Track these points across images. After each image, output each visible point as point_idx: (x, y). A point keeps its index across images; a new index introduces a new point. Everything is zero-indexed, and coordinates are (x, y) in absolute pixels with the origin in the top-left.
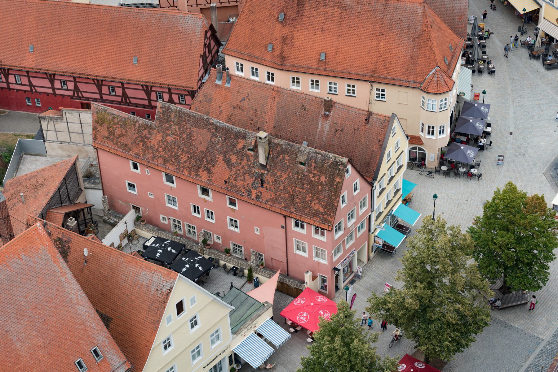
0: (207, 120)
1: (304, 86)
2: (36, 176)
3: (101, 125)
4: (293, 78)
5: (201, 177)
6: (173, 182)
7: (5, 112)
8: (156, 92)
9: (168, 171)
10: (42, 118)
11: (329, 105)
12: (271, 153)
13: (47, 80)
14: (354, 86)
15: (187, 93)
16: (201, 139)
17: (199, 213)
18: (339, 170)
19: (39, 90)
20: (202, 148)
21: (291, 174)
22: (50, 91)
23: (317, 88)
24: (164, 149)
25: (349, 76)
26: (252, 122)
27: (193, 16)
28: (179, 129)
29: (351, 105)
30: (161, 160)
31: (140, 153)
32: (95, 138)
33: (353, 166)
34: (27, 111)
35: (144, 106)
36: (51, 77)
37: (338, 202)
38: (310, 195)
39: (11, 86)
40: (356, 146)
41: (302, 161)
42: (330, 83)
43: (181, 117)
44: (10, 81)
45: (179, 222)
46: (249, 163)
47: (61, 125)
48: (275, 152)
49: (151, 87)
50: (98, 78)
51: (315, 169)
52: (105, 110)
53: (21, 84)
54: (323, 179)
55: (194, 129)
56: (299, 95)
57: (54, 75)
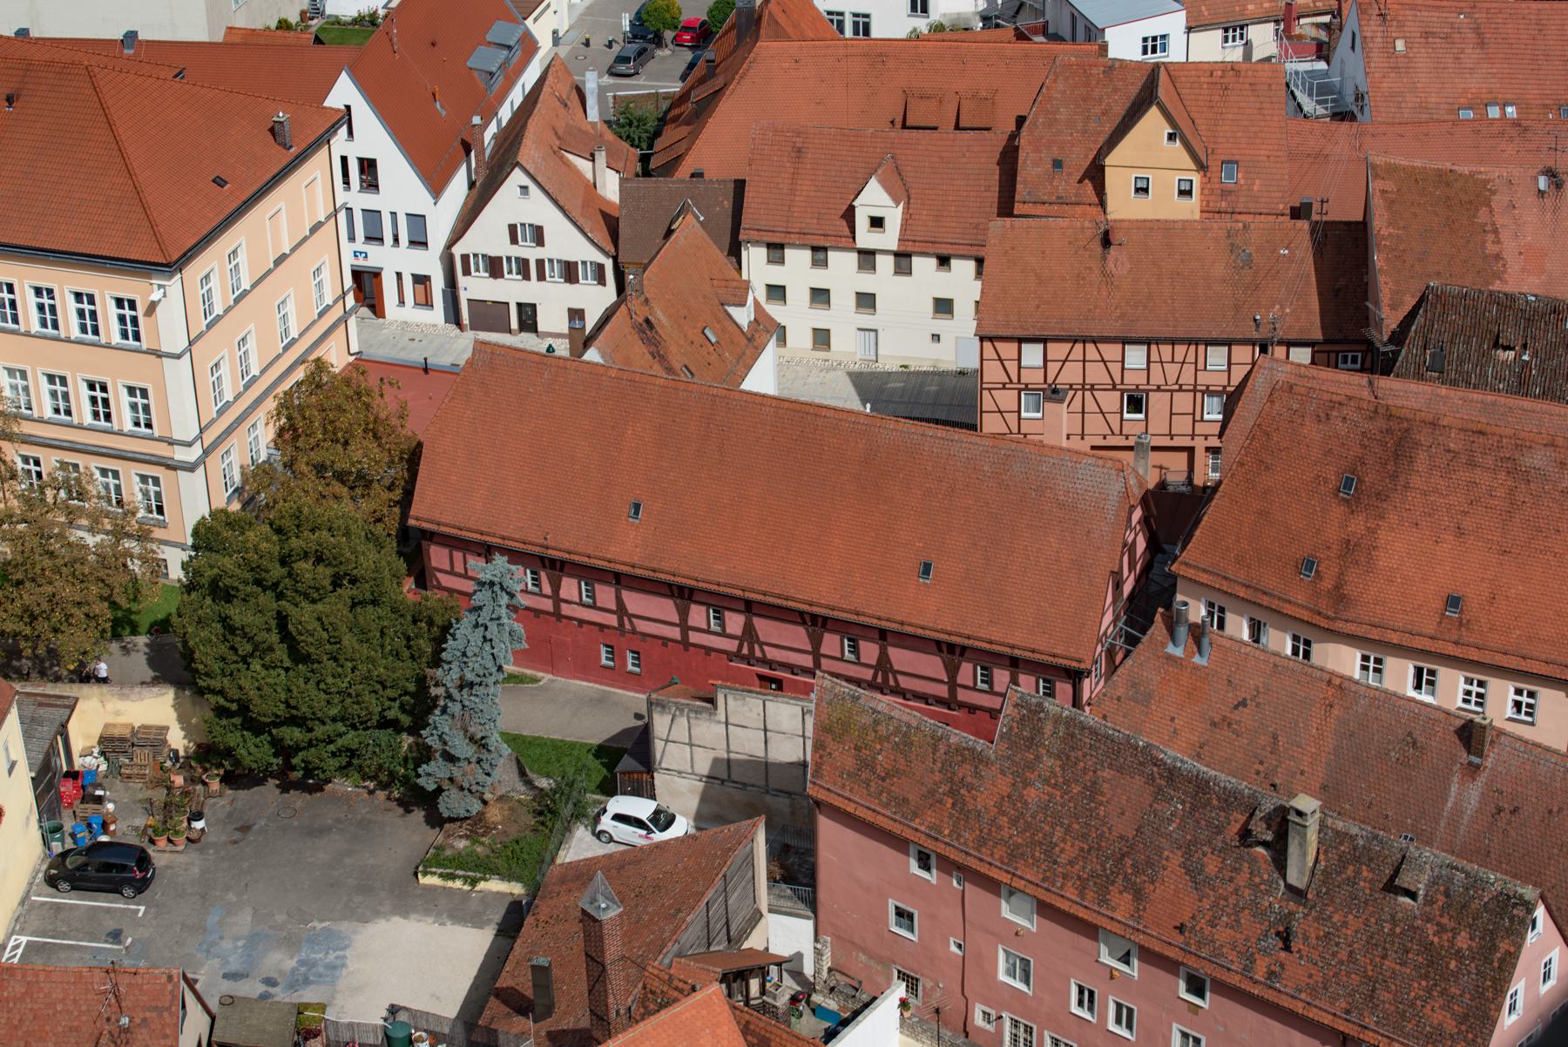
2: (638, 862)
5: (1114, 909)
7: (535, 680)
12: (1321, 857)
16: (1125, 800)
17: (1091, 1009)
18: (1512, 919)
19: (643, 626)
20: (1124, 827)
22: (675, 633)
24: (1014, 822)
26: (1261, 768)
27: (1100, 462)
28: (1063, 768)
29: (1546, 743)
30: (1000, 852)
33: (1548, 909)
36: (683, 594)
37: (1499, 1009)
38: (1424, 983)
39: (566, 609)
43: (1072, 735)
44: (563, 594)
45: (1029, 1030)
46: (1257, 880)
47: (709, 731)
48: (1333, 855)
52: (856, 699)
53: (594, 607)
54: (1463, 941)
55: (1106, 773)
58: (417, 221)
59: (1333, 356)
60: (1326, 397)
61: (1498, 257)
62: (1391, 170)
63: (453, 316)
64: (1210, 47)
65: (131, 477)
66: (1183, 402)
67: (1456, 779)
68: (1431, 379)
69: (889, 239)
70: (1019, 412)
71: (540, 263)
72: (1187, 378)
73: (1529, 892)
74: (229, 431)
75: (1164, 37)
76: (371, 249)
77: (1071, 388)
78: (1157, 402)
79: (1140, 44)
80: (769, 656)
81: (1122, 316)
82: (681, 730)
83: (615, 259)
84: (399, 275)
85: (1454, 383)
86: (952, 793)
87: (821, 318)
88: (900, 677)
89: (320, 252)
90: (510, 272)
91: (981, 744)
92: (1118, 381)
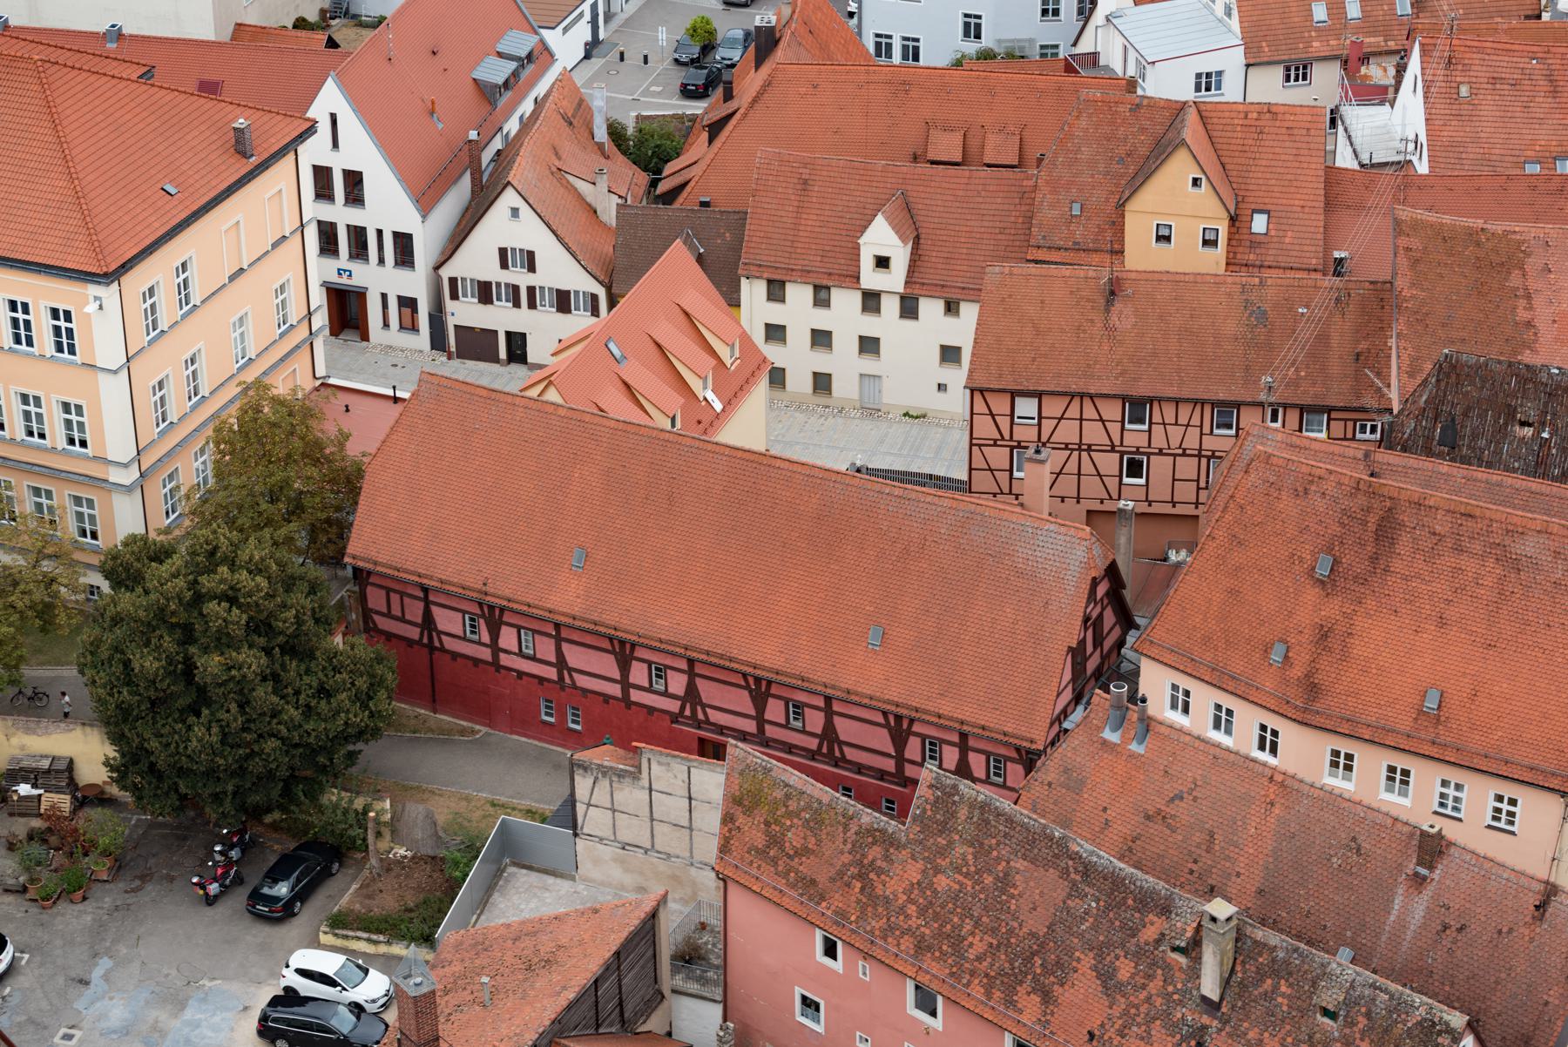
0: (1062, 843)
1: (1366, 782)
2: (535, 934)
3: (749, 812)
4: (1336, 753)
5: (1021, 1012)
6: (933, 1014)
7: (473, 732)
8: (923, 738)
9: (924, 979)
10: (579, 766)
11: (1432, 848)
12: (1238, 968)
13: (612, 657)
14: (1513, 802)
15: (1014, 755)
16: (1038, 895)
19: (583, 681)
20: (1035, 923)
21: (1289, 1040)
22: (615, 690)
23: (1403, 794)
24: (922, 912)
25: (1504, 770)
26: (1195, 867)
27: (1063, 529)
28: (975, 857)
29: (1500, 857)
30: (907, 943)
31: (849, 911)
32: (724, 849)
34: (540, 740)
35: (882, 775)
36: (624, 651)
39: (504, 660)
40: (1497, 983)
41: (1331, 1007)
42: (1445, 783)
43: (987, 822)
44: (502, 643)
46: (1170, 989)
47: (631, 796)
48: (1251, 968)
49: (912, 721)
50: (758, 672)
51: (1363, 1033)
52: (767, 771)
53: (533, 658)
55: (1020, 864)
56: (1346, 805)
57: (633, 646)
58: (404, 243)
59: (1350, 424)
60: (1304, 469)
61: (1529, 324)
62: (1416, 225)
63: (438, 342)
64: (1269, 87)
65: (62, 496)
66: (1187, 467)
67: (1400, 891)
68: (1440, 456)
69: (893, 281)
70: (1011, 471)
71: (531, 290)
72: (1192, 442)
73: (1457, 1020)
74: (168, 454)
75: (1220, 73)
76: (356, 267)
77: (1066, 448)
78: (1159, 468)
79: (1193, 80)
80: (712, 720)
81: (1122, 374)
82: (602, 795)
83: (609, 289)
84: (384, 296)
85: (1465, 461)
86: (861, 876)
87: (821, 361)
88: (845, 749)
89: (285, 265)
90: (499, 299)
91: (893, 825)
92: (1117, 443)
